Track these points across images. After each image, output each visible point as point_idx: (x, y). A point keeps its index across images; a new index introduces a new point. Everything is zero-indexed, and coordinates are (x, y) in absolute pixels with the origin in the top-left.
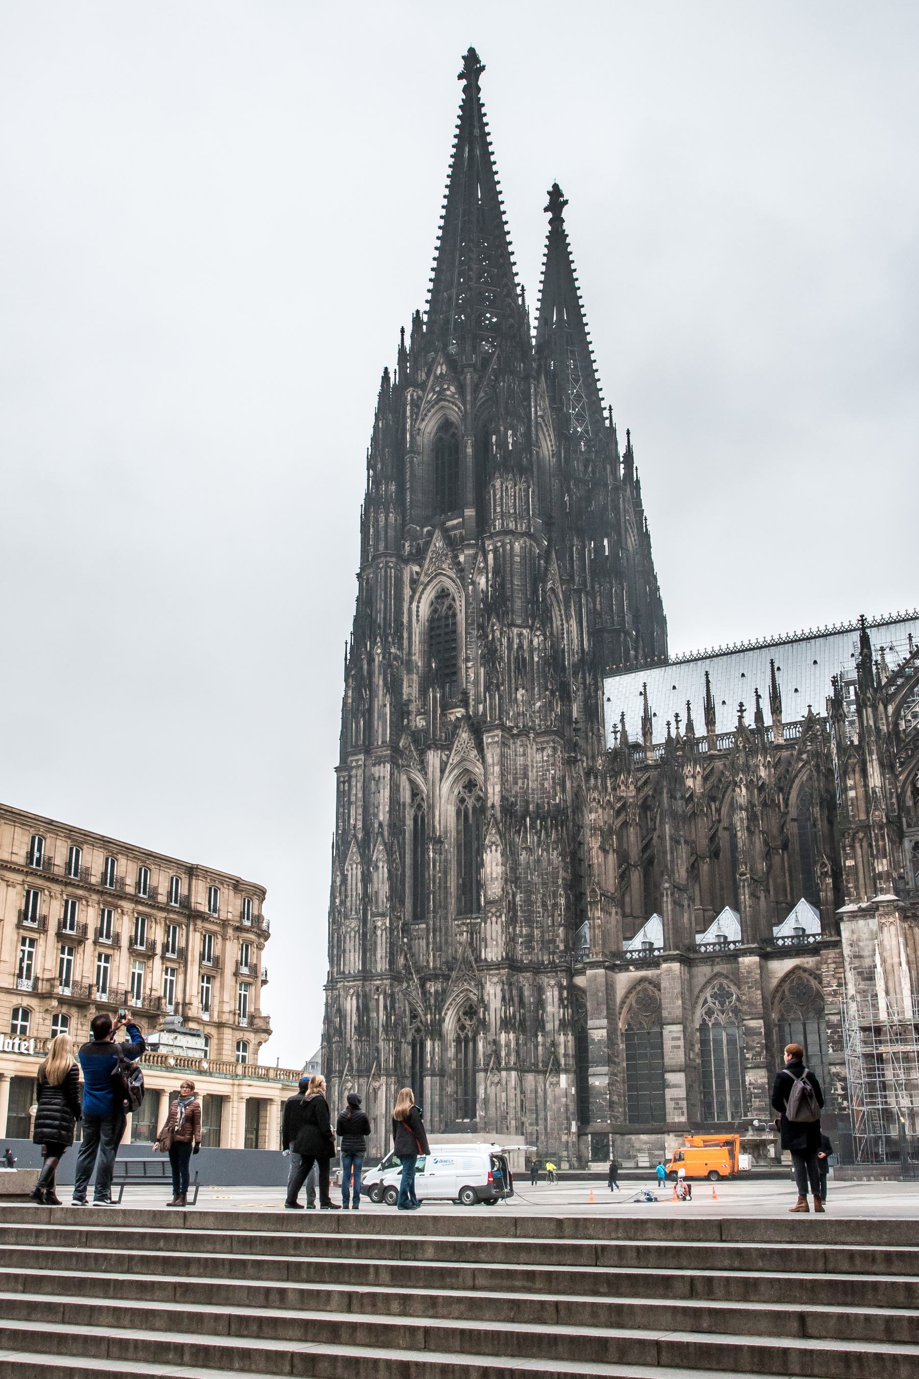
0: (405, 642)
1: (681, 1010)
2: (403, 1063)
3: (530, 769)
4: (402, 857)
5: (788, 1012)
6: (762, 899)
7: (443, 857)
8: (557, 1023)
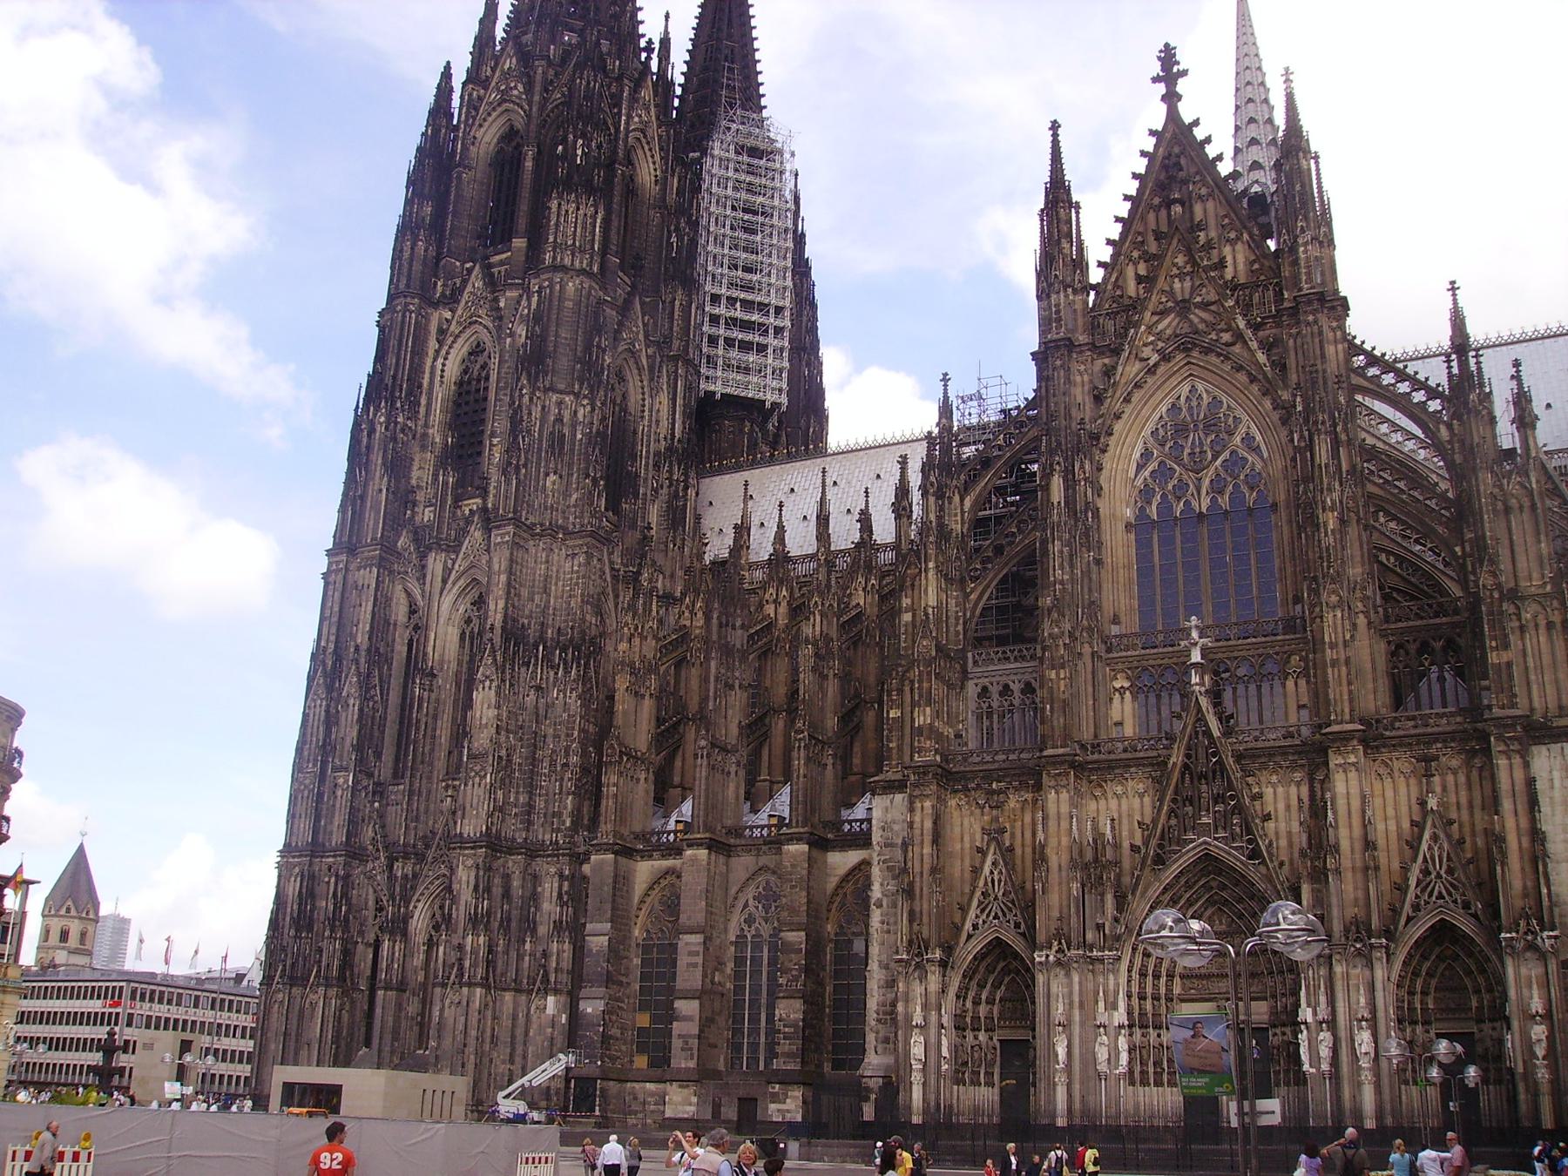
0: (422, 410)
2: (356, 970)
4: (384, 694)
5: (849, 922)
6: (830, 767)
7: (433, 696)
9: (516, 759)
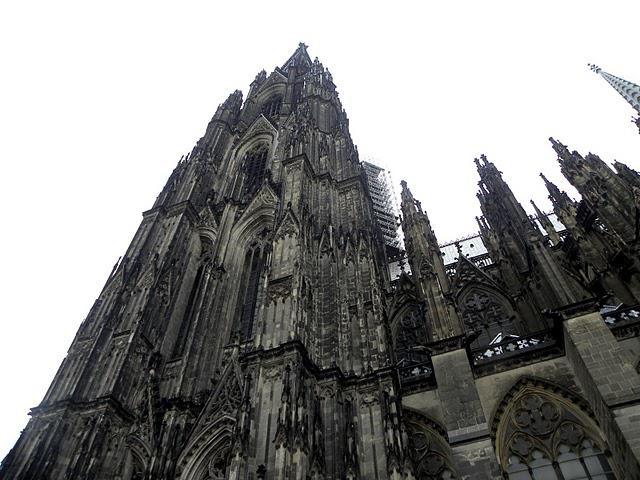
8: (382, 460)
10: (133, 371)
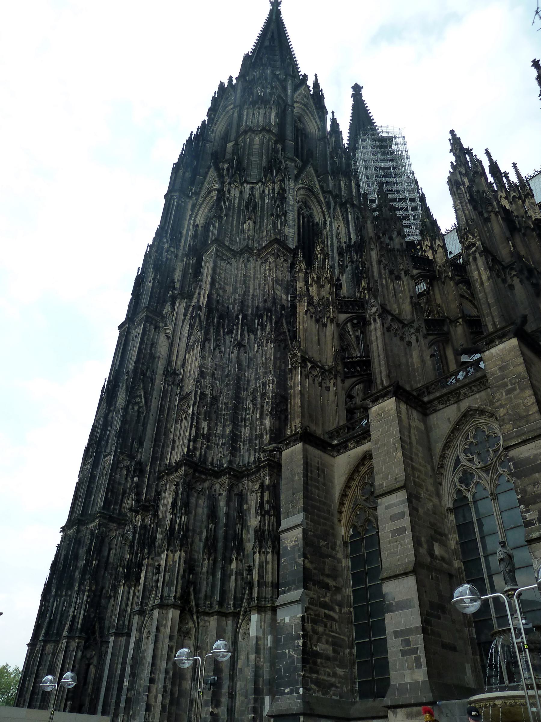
1: (402, 466)
3: (252, 280)
9: (222, 400)
10: (120, 484)
